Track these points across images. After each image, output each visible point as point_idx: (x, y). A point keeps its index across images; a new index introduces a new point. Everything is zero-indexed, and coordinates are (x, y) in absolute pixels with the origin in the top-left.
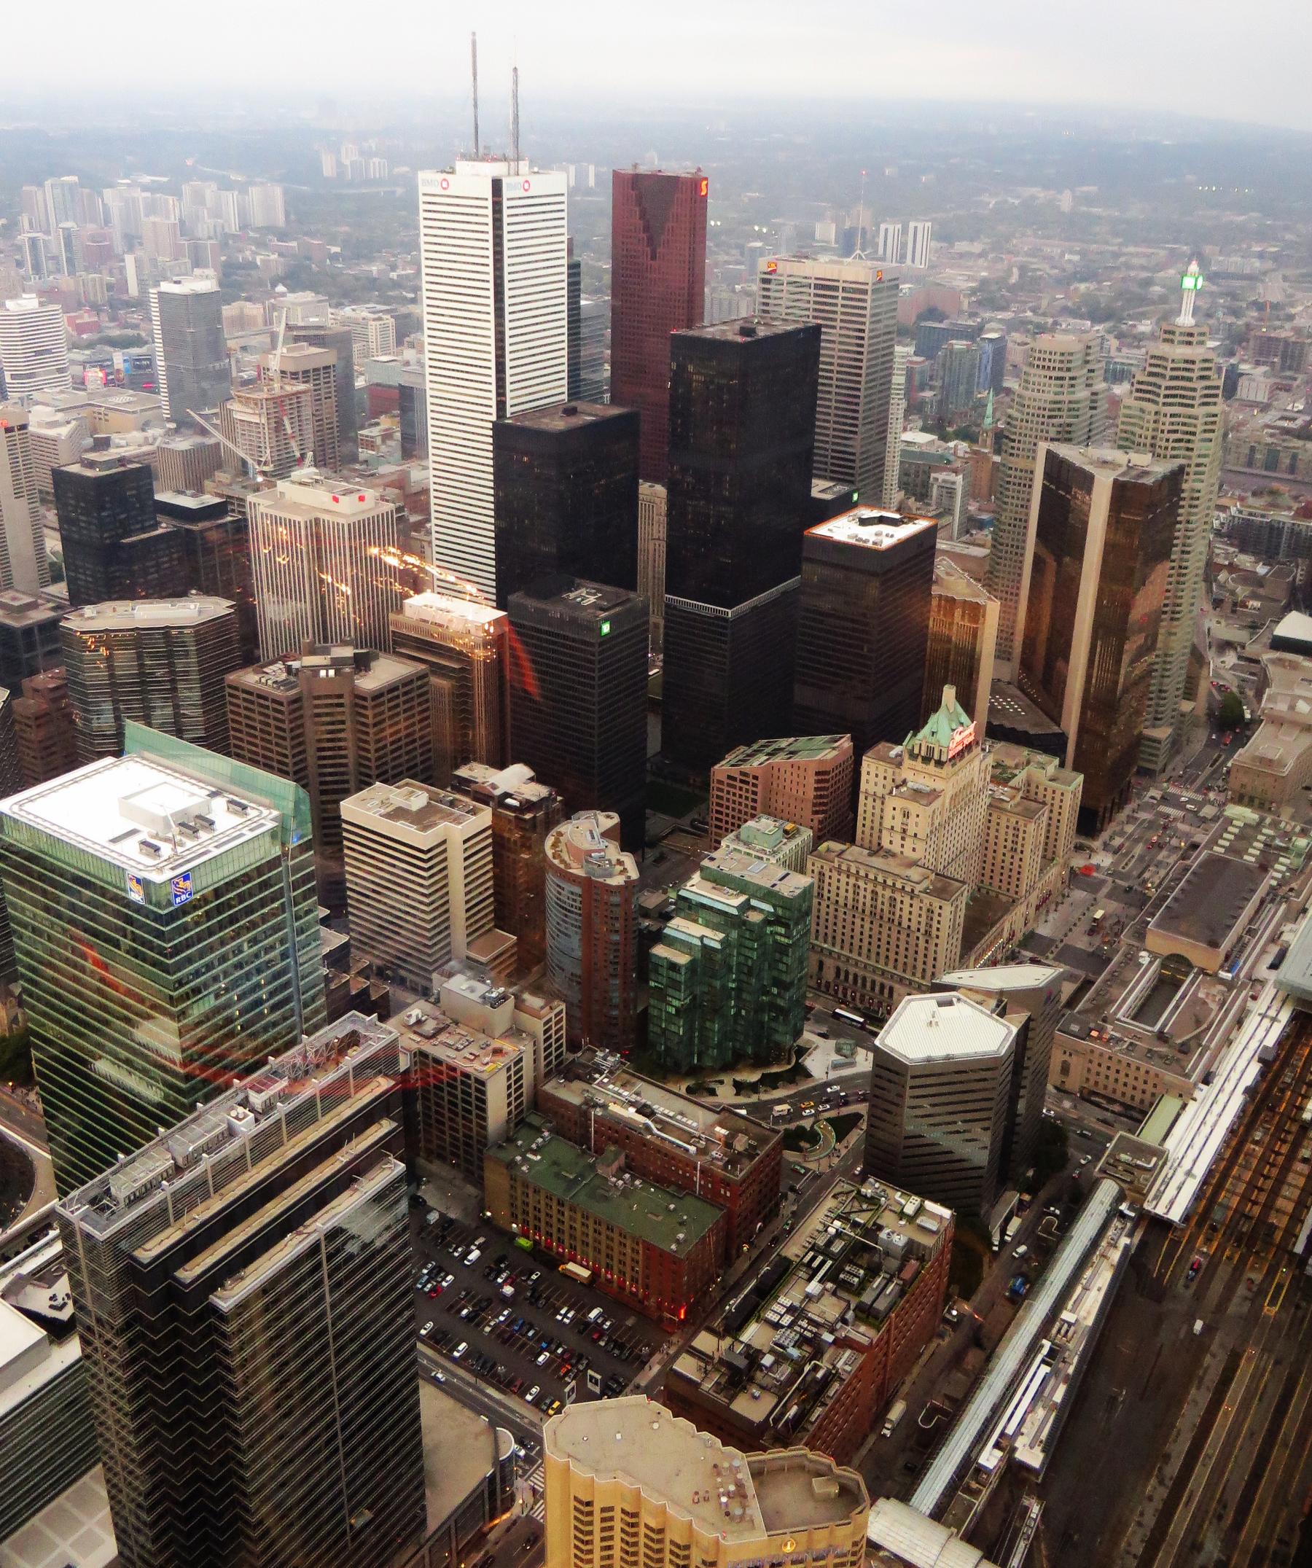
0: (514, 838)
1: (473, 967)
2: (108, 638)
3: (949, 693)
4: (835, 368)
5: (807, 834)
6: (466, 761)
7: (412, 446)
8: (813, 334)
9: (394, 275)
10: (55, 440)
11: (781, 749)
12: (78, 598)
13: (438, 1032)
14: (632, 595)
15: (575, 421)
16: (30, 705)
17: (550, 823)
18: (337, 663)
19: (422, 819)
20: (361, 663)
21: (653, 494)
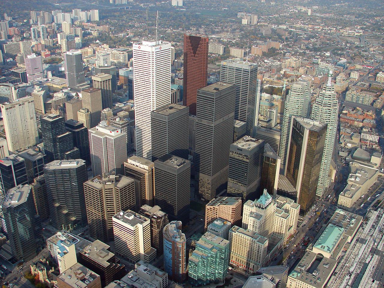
3: (265, 191)
4: (241, 83)
9: (127, 37)
11: (224, 201)
13: (137, 280)
14: (186, 161)
15: (172, 111)
19: (133, 223)
20: (117, 180)
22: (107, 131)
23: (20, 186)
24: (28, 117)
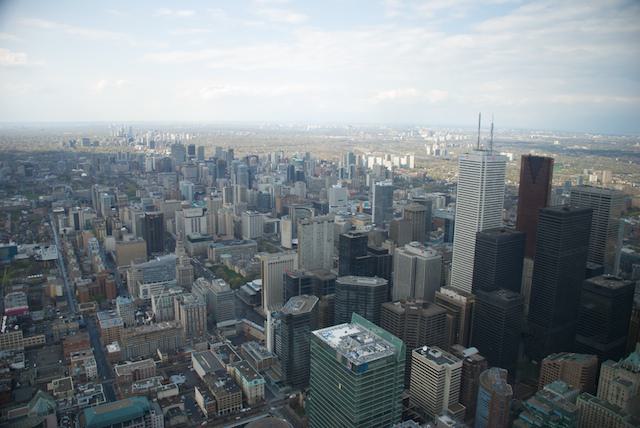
0: (468, 373)
1: (449, 414)
2: (348, 288)
5: (577, 391)
6: (455, 343)
7: (448, 238)
8: (590, 212)
10: (340, 226)
12: (341, 275)
16: (322, 304)
17: (482, 370)
18: (417, 305)
19: (439, 361)
20: (425, 306)
21: (529, 264)
22: (418, 251)
23: (306, 296)
24: (326, 238)
